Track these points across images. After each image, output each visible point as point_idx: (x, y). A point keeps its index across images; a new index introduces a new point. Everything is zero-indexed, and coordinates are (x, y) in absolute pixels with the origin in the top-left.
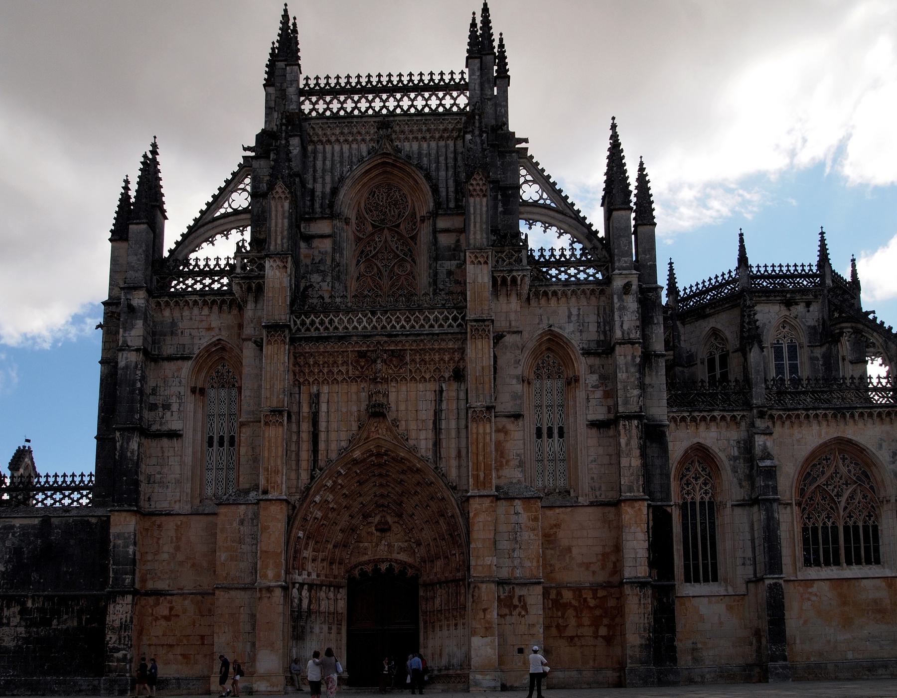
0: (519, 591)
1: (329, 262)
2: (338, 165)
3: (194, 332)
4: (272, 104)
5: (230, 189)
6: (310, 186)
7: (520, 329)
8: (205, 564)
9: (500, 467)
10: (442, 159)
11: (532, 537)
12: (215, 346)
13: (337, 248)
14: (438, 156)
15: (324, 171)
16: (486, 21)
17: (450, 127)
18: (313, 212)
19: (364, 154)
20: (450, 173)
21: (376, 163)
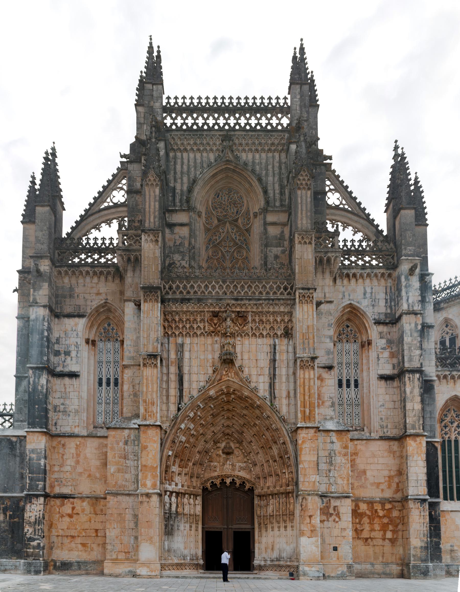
0: (334, 503)
1: (187, 245)
2: (193, 169)
3: (87, 296)
4: (142, 120)
5: (111, 186)
6: (172, 185)
7: (332, 300)
8: (98, 475)
9: (319, 406)
10: (270, 167)
11: (344, 461)
12: (103, 307)
13: (192, 234)
14: (267, 165)
15: (182, 173)
16: (303, 59)
17: (276, 142)
18: (175, 205)
19: (213, 161)
20: (276, 178)
21: (221, 168)
